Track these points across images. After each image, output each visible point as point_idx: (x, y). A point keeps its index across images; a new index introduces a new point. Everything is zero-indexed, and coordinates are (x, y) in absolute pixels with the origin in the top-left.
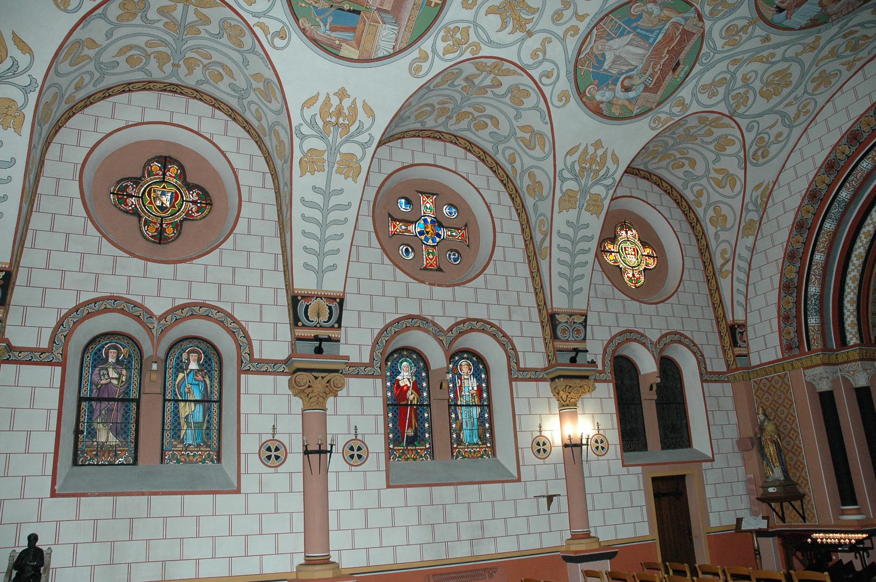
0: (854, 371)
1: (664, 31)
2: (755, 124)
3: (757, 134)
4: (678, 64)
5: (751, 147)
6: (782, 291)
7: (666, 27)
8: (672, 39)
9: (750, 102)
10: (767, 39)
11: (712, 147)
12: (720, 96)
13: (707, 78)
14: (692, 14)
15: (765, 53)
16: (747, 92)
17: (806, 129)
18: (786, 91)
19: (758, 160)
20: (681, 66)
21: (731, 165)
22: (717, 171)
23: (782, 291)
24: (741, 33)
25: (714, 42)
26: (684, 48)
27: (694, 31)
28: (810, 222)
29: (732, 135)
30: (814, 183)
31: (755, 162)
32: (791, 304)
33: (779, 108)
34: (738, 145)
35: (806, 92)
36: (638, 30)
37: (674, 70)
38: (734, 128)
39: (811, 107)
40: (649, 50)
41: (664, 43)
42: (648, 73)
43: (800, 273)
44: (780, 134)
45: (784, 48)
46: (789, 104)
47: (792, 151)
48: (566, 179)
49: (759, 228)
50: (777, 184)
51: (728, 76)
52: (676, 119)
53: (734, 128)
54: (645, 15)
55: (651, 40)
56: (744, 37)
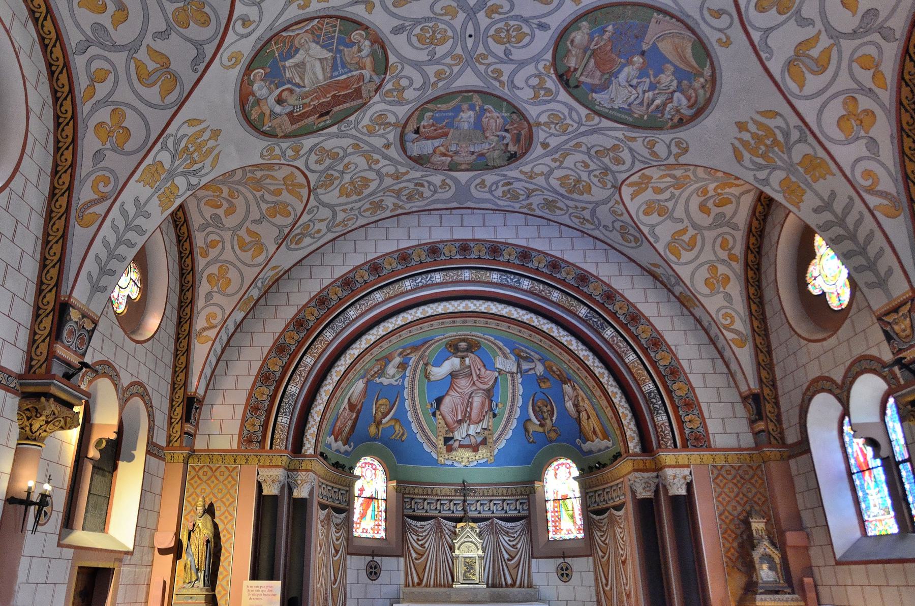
1: (350, 75)
2: (316, 210)
3: (310, 221)
4: (327, 113)
5: (298, 227)
7: (354, 73)
8: (346, 88)
9: (329, 190)
10: (387, 146)
11: (264, 207)
12: (319, 168)
13: (330, 144)
14: (378, 82)
15: (376, 157)
16: (336, 178)
17: (334, 239)
18: (354, 198)
19: (291, 243)
20: (328, 117)
21: (268, 234)
22: (249, 232)
24: (382, 127)
25: (363, 117)
26: (345, 103)
27: (364, 96)
28: (311, 324)
29: (293, 208)
30: (327, 290)
31: (289, 243)
33: (337, 209)
34: (290, 220)
35: (360, 208)
36: (338, 55)
37: (321, 115)
38: (302, 202)
39: (350, 223)
40: (325, 80)
41: (339, 85)
42: (304, 101)
44: (318, 231)
45: (388, 162)
46: (344, 211)
47: (313, 251)
48: (167, 149)
50: (287, 274)
51: (341, 154)
52: (283, 161)
53: (302, 202)
54: (355, 48)
55: (336, 73)
56: (381, 131)
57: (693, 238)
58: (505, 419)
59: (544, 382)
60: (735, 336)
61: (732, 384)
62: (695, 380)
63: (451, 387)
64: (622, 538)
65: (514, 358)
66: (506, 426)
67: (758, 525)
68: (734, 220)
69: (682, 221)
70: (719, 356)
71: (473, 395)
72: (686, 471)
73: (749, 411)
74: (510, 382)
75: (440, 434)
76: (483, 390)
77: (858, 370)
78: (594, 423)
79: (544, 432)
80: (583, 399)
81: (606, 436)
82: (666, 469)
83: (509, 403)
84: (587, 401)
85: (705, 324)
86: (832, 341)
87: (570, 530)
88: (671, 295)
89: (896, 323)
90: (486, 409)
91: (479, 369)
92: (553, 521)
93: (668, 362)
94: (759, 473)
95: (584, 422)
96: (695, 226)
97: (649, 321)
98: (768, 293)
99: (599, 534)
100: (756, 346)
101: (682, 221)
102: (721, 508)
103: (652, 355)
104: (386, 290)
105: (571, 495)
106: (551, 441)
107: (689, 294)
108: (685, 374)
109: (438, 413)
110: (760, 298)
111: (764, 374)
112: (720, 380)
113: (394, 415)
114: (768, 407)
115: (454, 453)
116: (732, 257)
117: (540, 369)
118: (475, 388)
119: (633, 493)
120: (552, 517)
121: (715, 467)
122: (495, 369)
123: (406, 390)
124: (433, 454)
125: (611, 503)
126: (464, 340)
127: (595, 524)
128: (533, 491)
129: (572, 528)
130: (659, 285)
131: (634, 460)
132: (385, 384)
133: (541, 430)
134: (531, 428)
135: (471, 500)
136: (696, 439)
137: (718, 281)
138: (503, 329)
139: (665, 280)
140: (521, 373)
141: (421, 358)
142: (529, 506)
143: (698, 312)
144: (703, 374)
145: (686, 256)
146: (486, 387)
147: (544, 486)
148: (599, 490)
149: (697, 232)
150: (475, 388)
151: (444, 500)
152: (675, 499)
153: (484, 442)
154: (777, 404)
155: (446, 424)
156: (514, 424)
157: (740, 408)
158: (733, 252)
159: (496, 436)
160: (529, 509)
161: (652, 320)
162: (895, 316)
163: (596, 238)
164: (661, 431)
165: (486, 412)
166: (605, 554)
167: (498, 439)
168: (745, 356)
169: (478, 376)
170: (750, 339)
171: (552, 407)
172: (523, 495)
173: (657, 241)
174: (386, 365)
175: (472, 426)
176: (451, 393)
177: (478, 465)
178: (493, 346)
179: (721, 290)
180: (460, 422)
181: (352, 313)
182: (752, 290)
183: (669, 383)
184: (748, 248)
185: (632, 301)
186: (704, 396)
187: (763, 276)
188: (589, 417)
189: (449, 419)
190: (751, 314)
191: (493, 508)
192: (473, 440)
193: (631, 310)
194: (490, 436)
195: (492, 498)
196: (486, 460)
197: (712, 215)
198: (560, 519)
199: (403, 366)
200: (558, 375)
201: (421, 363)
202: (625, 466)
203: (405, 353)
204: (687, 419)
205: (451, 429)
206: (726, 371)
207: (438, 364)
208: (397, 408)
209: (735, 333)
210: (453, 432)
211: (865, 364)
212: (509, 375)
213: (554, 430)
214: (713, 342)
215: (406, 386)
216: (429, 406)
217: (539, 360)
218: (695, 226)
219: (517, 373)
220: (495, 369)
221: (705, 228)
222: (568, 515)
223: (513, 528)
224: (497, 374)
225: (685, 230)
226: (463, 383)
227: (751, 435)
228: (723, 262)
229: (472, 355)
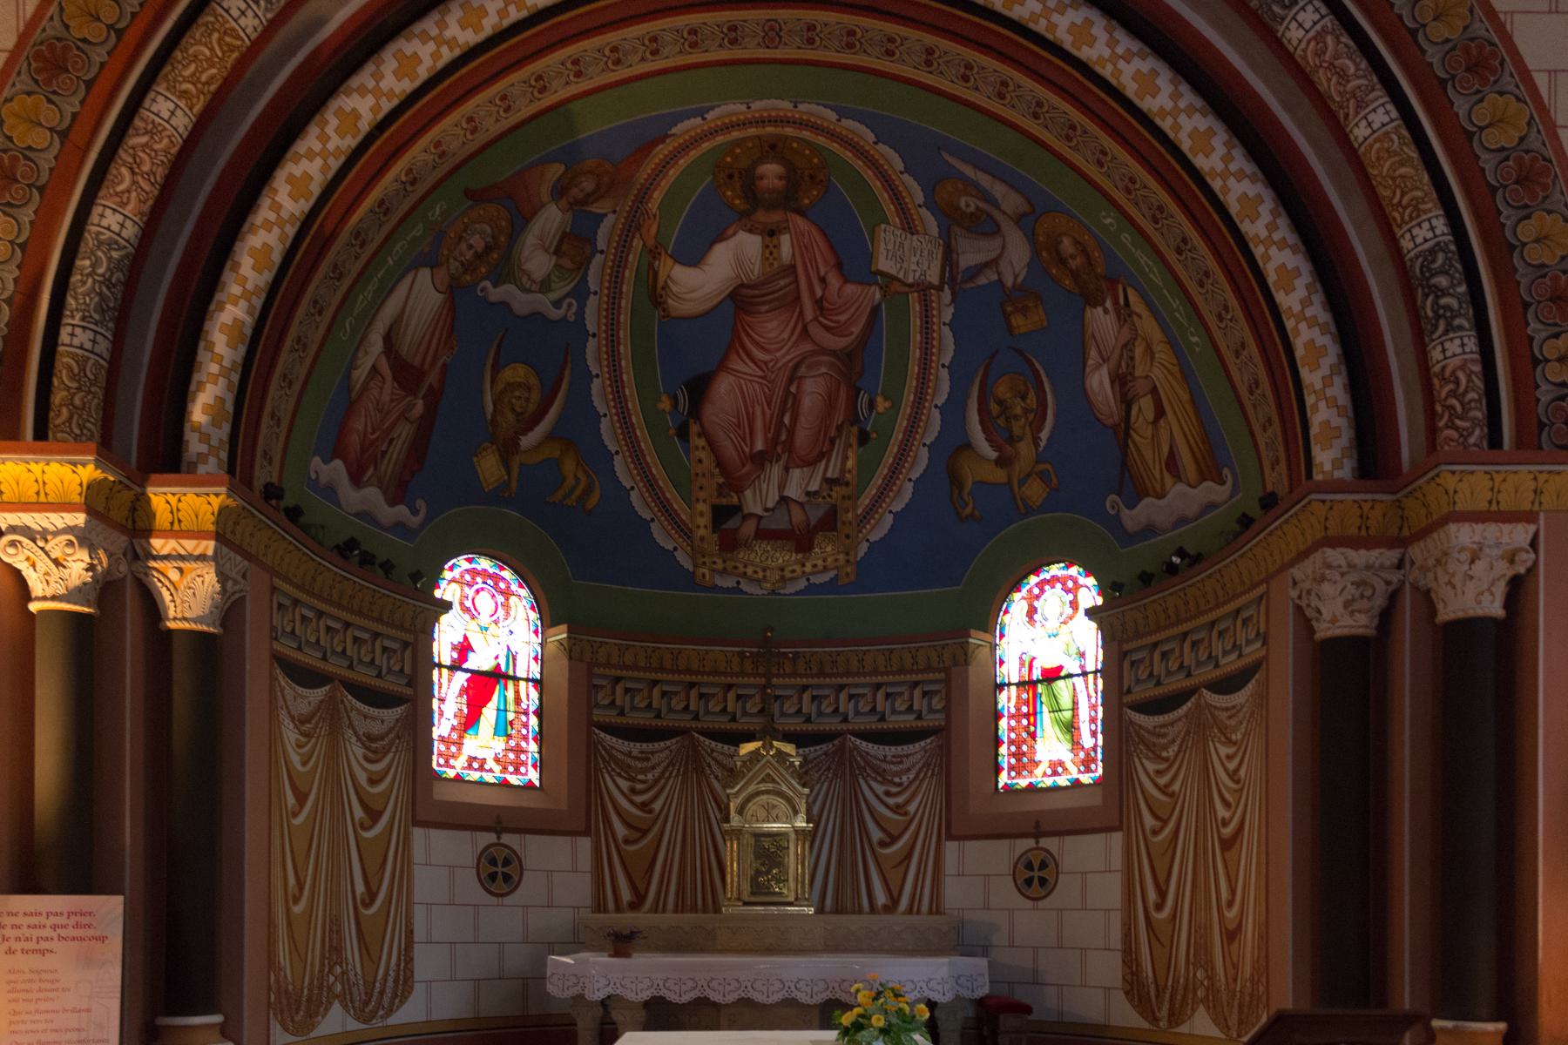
58: (894, 448)
66: (894, 471)
75: (702, 495)
78: (1178, 431)
81: (1210, 470)
82: (1453, 527)
87: (1061, 763)
90: (839, 418)
92: (1011, 742)
99: (1151, 767)
109: (694, 428)
115: (742, 554)
124: (679, 555)
128: (963, 657)
133: (1000, 475)
134: (973, 473)
135: (786, 687)
147: (994, 647)
151: (708, 684)
152: (1468, 628)
153: (829, 522)
155: (719, 464)
156: (921, 461)
159: (865, 501)
171: (1043, 404)
172: (934, 670)
175: (796, 474)
177: (811, 589)
180: (760, 460)
189: (729, 450)
191: (845, 706)
195: (845, 680)
196: (832, 574)
200: (1075, 275)
205: (734, 483)
210: (740, 491)
223: (899, 759)
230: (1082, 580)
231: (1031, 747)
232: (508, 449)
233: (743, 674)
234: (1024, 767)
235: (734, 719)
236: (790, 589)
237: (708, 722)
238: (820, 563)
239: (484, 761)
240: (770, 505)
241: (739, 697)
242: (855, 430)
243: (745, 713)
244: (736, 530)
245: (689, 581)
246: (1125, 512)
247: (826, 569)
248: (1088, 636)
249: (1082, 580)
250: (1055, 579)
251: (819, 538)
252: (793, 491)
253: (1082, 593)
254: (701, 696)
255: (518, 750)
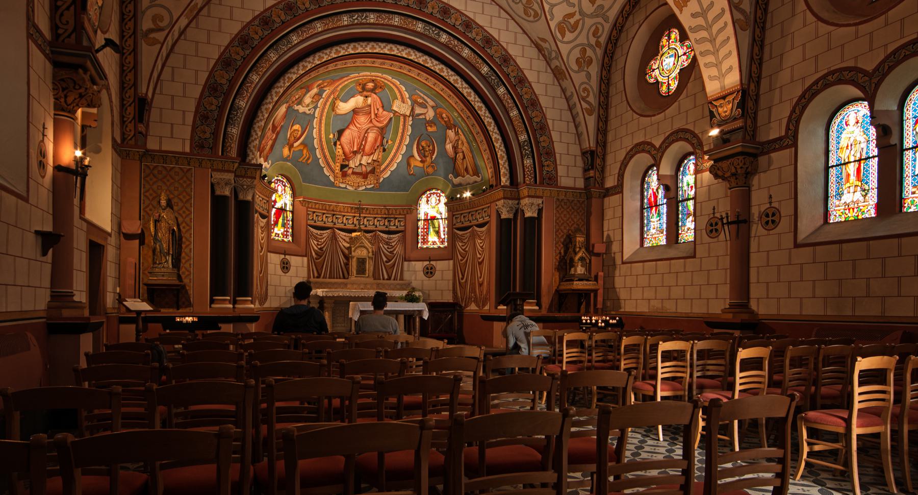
0: (248, 186)
6: (206, 90)
23: (206, 90)
28: (256, 43)
30: (270, 11)
32: (214, 107)
43: (232, 82)
49: (195, 17)
57: (577, 22)
58: (392, 154)
59: (431, 126)
60: (588, 107)
61: (577, 143)
62: (555, 136)
63: (352, 122)
64: (482, 247)
65: (410, 103)
67: (580, 239)
68: (607, 14)
69: (574, 6)
70: (572, 121)
71: (369, 131)
72: (540, 201)
73: (584, 163)
74: (401, 123)
75: (338, 161)
76: (378, 127)
77: (674, 138)
79: (423, 167)
80: (462, 142)
83: (398, 141)
84: (466, 144)
85: (568, 94)
86: (660, 117)
88: (548, 68)
89: (722, 107)
90: (378, 144)
91: (378, 109)
93: (540, 119)
94: (583, 205)
95: (459, 161)
96: (581, 13)
97: (531, 85)
98: (616, 77)
100: (599, 116)
101: (574, 6)
102: (557, 227)
103: (530, 112)
104: (326, 21)
105: (438, 216)
106: (428, 175)
107: (564, 68)
108: (550, 131)
109: (338, 143)
110: (608, 80)
111: (600, 136)
112: (571, 138)
113: (305, 138)
114: (598, 161)
115: (348, 178)
116: (598, 44)
117: (430, 114)
118: (371, 125)
119: (499, 215)
120: (422, 232)
121: (558, 199)
122: (391, 110)
123: (316, 120)
124: (330, 177)
125: (475, 222)
126: (373, 81)
127: (458, 237)
129: (436, 239)
130: (541, 57)
131: (505, 190)
132: (301, 111)
133: (421, 165)
134: (413, 163)
136: (550, 179)
137: (584, 61)
138: (413, 75)
139: (547, 54)
140: (413, 116)
141: (333, 92)
142: (405, 223)
143: (566, 83)
144: (561, 132)
145: (569, 36)
146: (380, 125)
148: (473, 211)
149: (581, 17)
150: (371, 125)
152: (531, 218)
153: (373, 171)
154: (604, 160)
155: (344, 153)
156: (399, 158)
157: (579, 159)
158: (600, 40)
159: (383, 167)
160: (405, 226)
161: (533, 84)
162: (722, 101)
163: (501, 7)
164: (528, 171)
165: (378, 147)
166: (464, 258)
167: (385, 169)
168: (592, 121)
169: (376, 115)
170: (597, 111)
173: (552, 20)
174: (305, 95)
175: (365, 158)
176: (351, 127)
177: (366, 189)
178: (395, 89)
179: (586, 69)
180: (355, 153)
181: (294, 38)
182: (604, 73)
183: (538, 136)
184: (610, 38)
185: (521, 67)
186: (559, 148)
187: (614, 63)
188: (464, 157)
189: (347, 149)
190: (600, 91)
191: (377, 223)
192: (364, 169)
193: (520, 74)
194: (378, 167)
196: (373, 186)
197: (596, 6)
198: (428, 234)
199: (319, 95)
201: (332, 96)
202: (499, 193)
203: (322, 86)
204: (546, 164)
205: (347, 158)
206: (575, 132)
207: (345, 100)
208: (307, 135)
209: (588, 104)
210: (349, 161)
211: (681, 135)
212: (402, 118)
213: (432, 166)
214: (570, 109)
215: (316, 116)
216: (331, 136)
217: (433, 107)
218: (581, 13)
219: (409, 117)
220: (391, 110)
221: (588, 16)
222: (435, 231)
224: (392, 115)
225: (571, 15)
226: (362, 119)
227: (583, 179)
228: (591, 46)
229: (375, 96)
230: (441, 194)
231: (427, 237)
232: (291, 146)
233: (348, 212)
234: (425, 242)
235: (345, 225)
236: (361, 189)
237: (338, 226)
238: (369, 182)
239: (279, 235)
240: (357, 165)
241: (347, 219)
242: (382, 148)
243: (348, 224)
244: (346, 171)
245: (332, 184)
246: (454, 179)
247: (371, 184)
248: (443, 208)
249: (441, 194)
250: (434, 193)
251: (369, 175)
252: (363, 162)
253: (441, 198)
254: (336, 218)
255: (287, 231)
